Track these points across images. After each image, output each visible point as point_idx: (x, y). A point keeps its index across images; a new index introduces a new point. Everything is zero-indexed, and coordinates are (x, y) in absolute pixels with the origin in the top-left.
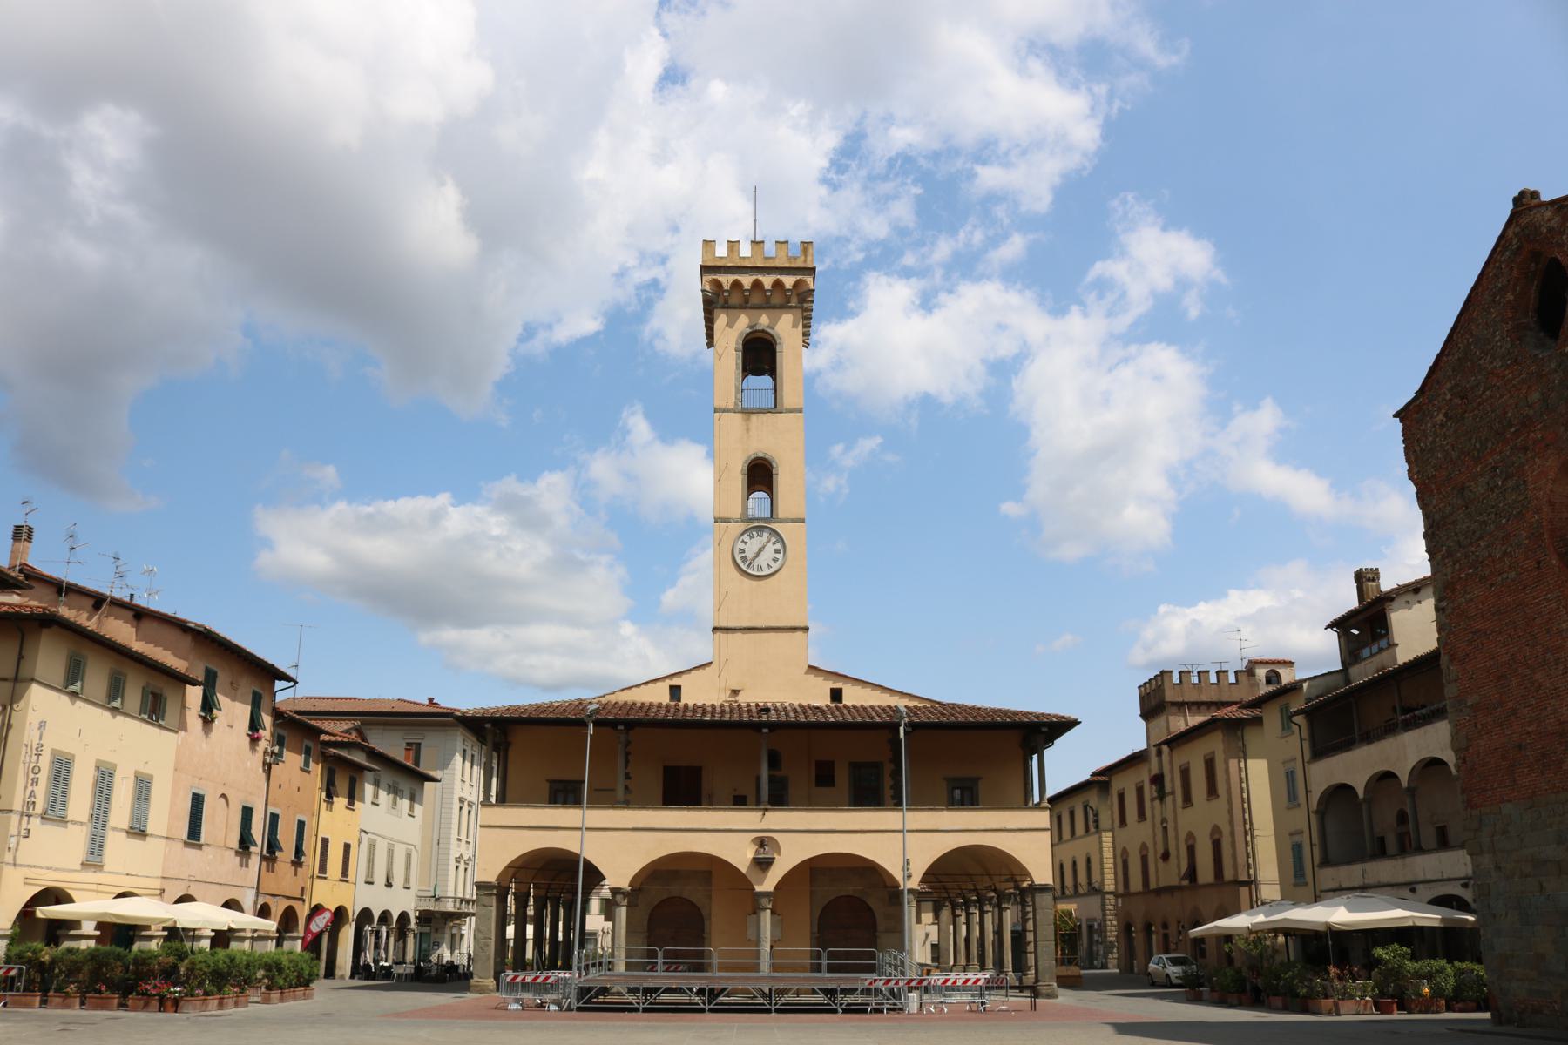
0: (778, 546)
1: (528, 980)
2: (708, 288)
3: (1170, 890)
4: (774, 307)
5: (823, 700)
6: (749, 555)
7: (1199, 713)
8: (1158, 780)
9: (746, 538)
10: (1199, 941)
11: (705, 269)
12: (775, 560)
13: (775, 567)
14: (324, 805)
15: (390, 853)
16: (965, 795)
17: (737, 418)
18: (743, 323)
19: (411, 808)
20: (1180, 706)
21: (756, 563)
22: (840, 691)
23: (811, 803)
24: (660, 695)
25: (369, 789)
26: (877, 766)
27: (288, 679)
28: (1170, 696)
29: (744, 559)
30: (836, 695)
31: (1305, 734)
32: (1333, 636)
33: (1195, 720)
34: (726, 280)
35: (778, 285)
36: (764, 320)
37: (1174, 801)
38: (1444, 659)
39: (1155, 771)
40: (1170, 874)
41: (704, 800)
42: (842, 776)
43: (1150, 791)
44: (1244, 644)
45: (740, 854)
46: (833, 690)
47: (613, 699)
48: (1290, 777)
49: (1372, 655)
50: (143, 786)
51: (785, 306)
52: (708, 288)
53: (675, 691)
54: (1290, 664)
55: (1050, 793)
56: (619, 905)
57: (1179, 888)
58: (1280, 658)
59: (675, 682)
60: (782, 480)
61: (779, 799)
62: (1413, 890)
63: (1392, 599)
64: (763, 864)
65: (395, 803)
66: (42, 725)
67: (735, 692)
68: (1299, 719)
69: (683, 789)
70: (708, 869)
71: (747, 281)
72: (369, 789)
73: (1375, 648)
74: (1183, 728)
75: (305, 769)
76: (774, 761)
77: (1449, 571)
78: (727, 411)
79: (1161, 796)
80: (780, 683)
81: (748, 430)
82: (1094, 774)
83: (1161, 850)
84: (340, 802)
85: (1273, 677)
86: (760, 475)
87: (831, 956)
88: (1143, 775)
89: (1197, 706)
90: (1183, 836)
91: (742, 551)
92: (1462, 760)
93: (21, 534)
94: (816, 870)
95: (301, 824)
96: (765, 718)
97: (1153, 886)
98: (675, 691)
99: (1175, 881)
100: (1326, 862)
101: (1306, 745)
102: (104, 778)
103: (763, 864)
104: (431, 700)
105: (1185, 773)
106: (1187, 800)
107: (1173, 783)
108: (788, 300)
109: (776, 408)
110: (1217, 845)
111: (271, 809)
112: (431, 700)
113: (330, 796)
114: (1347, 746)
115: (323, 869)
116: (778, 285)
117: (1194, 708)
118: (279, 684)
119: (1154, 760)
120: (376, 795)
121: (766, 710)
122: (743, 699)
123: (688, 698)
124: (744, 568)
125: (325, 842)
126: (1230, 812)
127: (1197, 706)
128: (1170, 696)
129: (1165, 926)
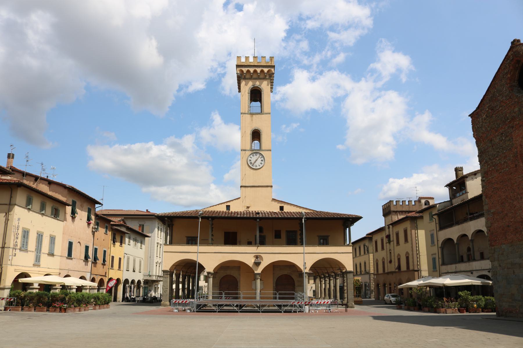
0: (262, 159)
1: (180, 302)
2: (239, 72)
3: (392, 273)
4: (261, 79)
5: (277, 210)
6: (253, 162)
7: (402, 215)
8: (388, 237)
9: (251, 156)
10: (401, 289)
11: (238, 66)
12: (261, 163)
13: (261, 166)
14: (112, 245)
15: (134, 261)
16: (324, 241)
17: (248, 116)
18: (250, 84)
19: (141, 246)
20: (396, 212)
21: (255, 165)
22: (283, 207)
23: (273, 244)
24: (223, 208)
25: (127, 240)
26: (295, 232)
27: (100, 204)
28: (393, 209)
29: (251, 163)
30: (282, 208)
31: (437, 222)
32: (447, 189)
33: (401, 217)
34: (245, 70)
35: (262, 71)
36: (257, 83)
37: (394, 244)
38: (484, 197)
39: (387, 234)
40: (392, 268)
41: (238, 243)
42: (284, 235)
43: (385, 240)
44: (418, 192)
45: (250, 261)
46: (280, 207)
47: (207, 210)
48: (432, 236)
49: (460, 196)
50: (53, 239)
51: (264, 79)
52: (239, 72)
53: (228, 207)
54: (433, 198)
55: (352, 241)
56: (210, 278)
57: (395, 272)
58: (429, 196)
59: (228, 204)
60: (264, 137)
61: (263, 243)
62: (472, 273)
63: (467, 177)
64: (257, 264)
65: (136, 244)
66: (19, 219)
67: (248, 207)
68: (435, 217)
69: (231, 239)
70: (239, 266)
71: (252, 70)
72: (127, 240)
73: (461, 193)
74: (397, 219)
75: (106, 233)
76: (261, 230)
77: (486, 167)
78: (245, 114)
79: (389, 242)
80: (263, 204)
81: (252, 120)
82: (367, 235)
83: (389, 260)
84: (118, 244)
85: (427, 203)
86: (256, 135)
87: (280, 294)
88: (384, 235)
89: (402, 212)
90: (396, 255)
91: (250, 160)
92: (489, 230)
93: (10, 156)
94: (275, 266)
95: (105, 252)
96: (258, 216)
97: (386, 271)
98: (228, 207)
99: (393, 270)
100: (443, 264)
101: (438, 225)
102: (40, 237)
103: (257, 264)
104: (147, 210)
105: (397, 235)
106: (398, 243)
107: (393, 238)
108: (266, 76)
109: (261, 113)
110: (407, 258)
111: (95, 247)
112: (147, 210)
113: (114, 242)
114: (451, 226)
115: (112, 266)
116: (262, 71)
117: (401, 213)
118: (97, 205)
119: (387, 230)
120: (129, 242)
121: (258, 213)
122: (250, 210)
123: (232, 209)
124: (251, 166)
125: (113, 257)
126: (412, 247)
127: (402, 212)
128: (393, 209)
129: (390, 284)
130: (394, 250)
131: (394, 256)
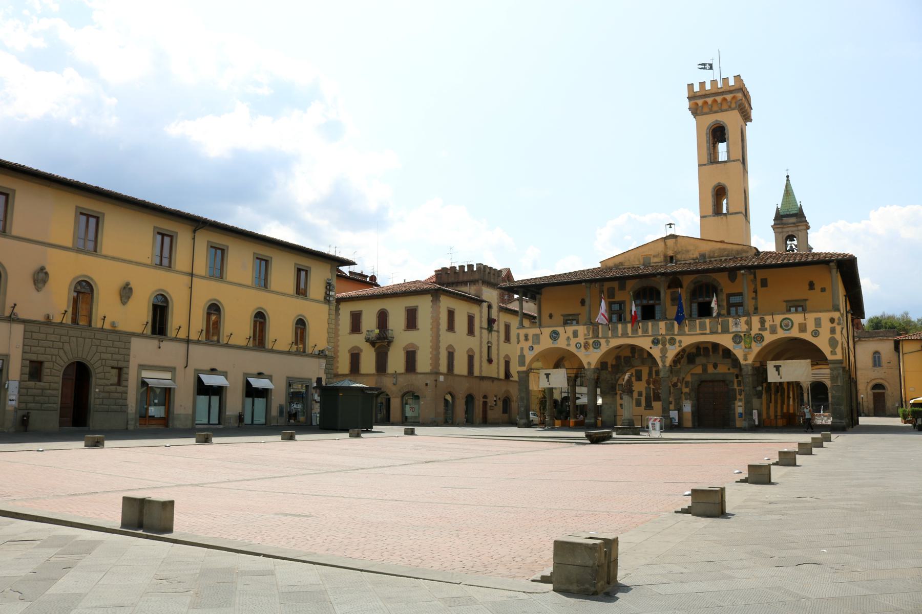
3: (492, 379)
37: (498, 336)
57: (498, 379)
79: (490, 328)
97: (477, 373)
130: (498, 345)
131: (498, 354)
